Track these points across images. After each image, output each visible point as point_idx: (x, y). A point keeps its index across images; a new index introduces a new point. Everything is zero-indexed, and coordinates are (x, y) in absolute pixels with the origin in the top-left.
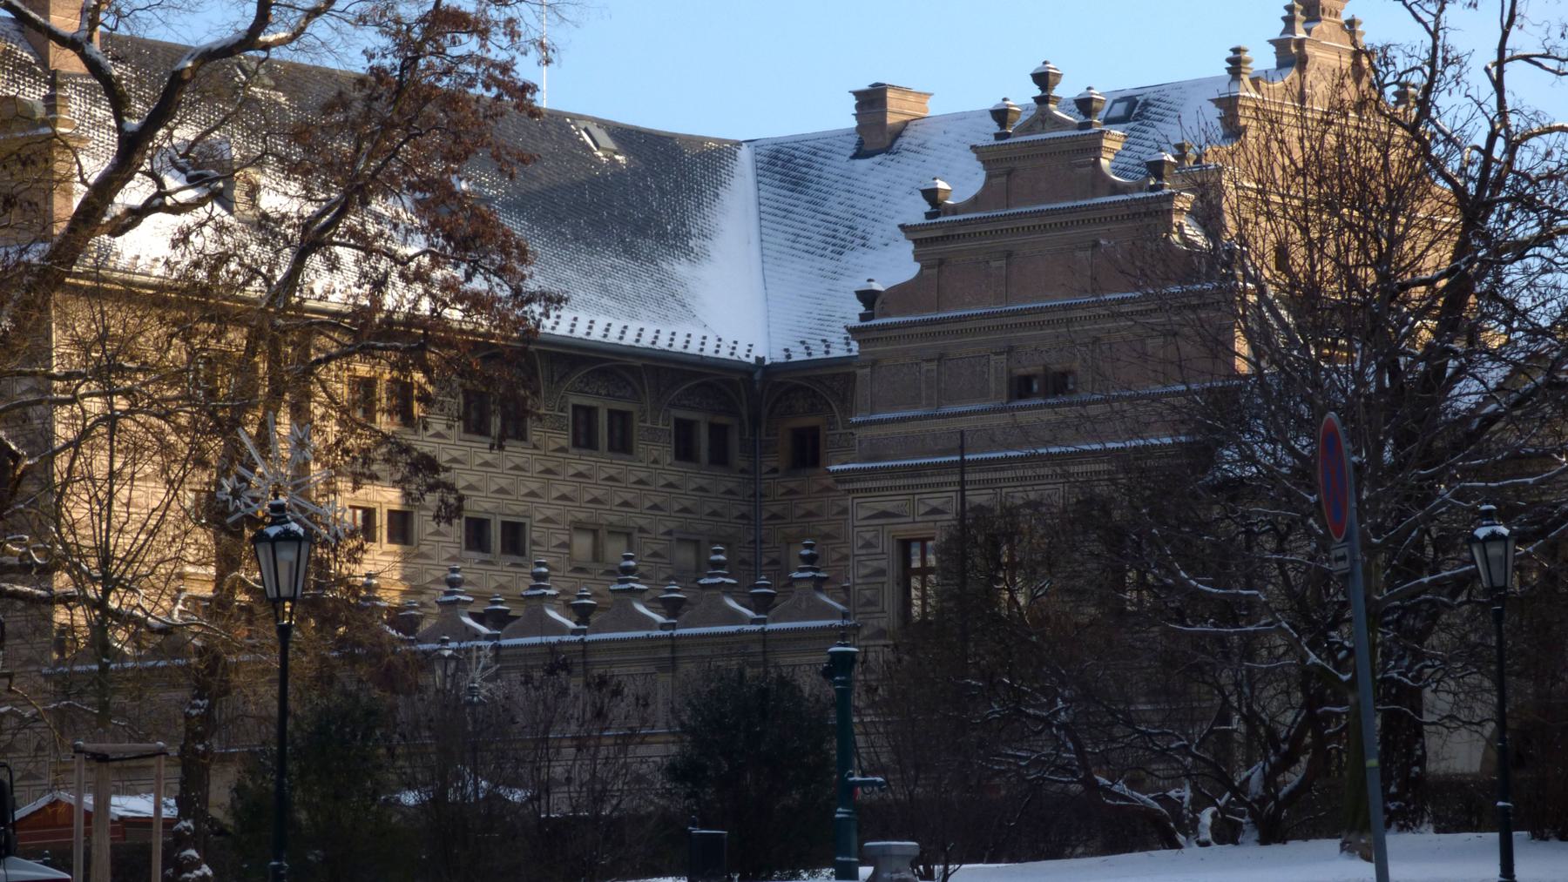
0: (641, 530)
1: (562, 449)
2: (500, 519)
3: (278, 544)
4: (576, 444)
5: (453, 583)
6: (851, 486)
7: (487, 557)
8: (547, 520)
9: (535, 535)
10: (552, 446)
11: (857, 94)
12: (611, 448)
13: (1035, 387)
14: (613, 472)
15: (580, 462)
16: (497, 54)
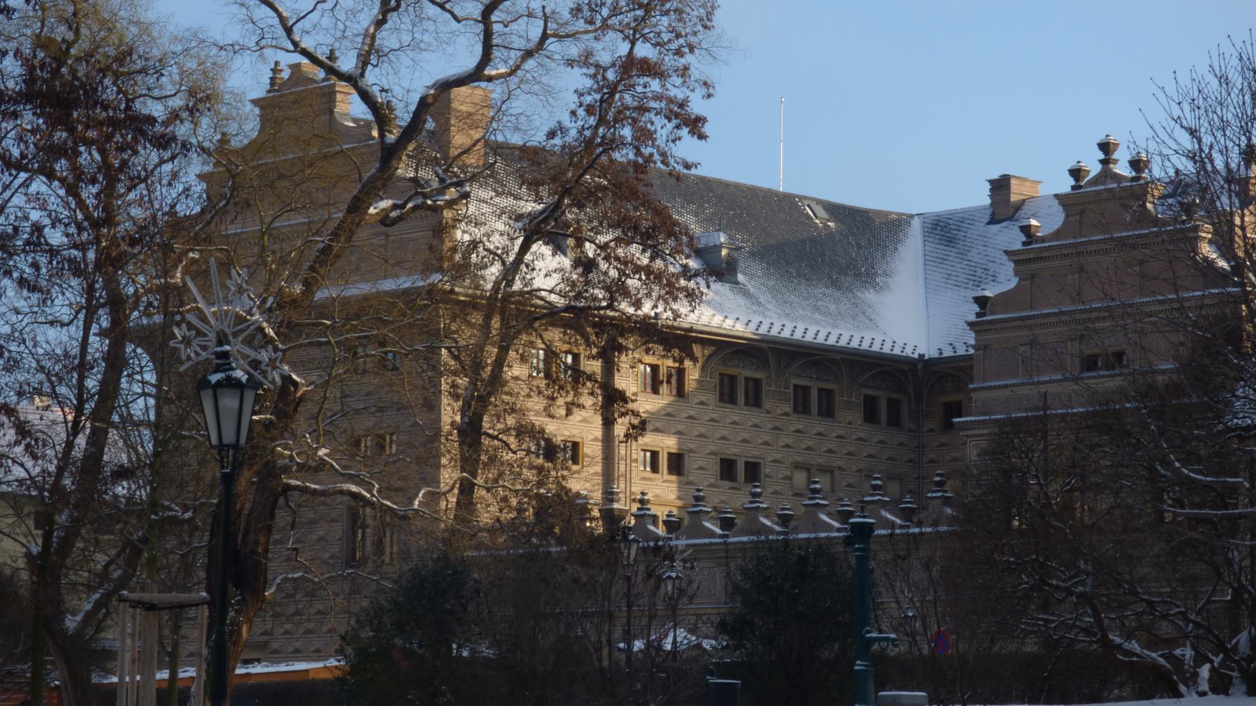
0: (840, 469)
1: (786, 414)
2: (743, 459)
3: (219, 391)
4: (796, 410)
5: (698, 499)
6: (969, 433)
7: (734, 485)
8: (776, 461)
9: (767, 471)
10: (779, 412)
11: (991, 182)
12: (820, 414)
13: (1100, 363)
14: (821, 430)
15: (799, 423)
16: (678, 93)
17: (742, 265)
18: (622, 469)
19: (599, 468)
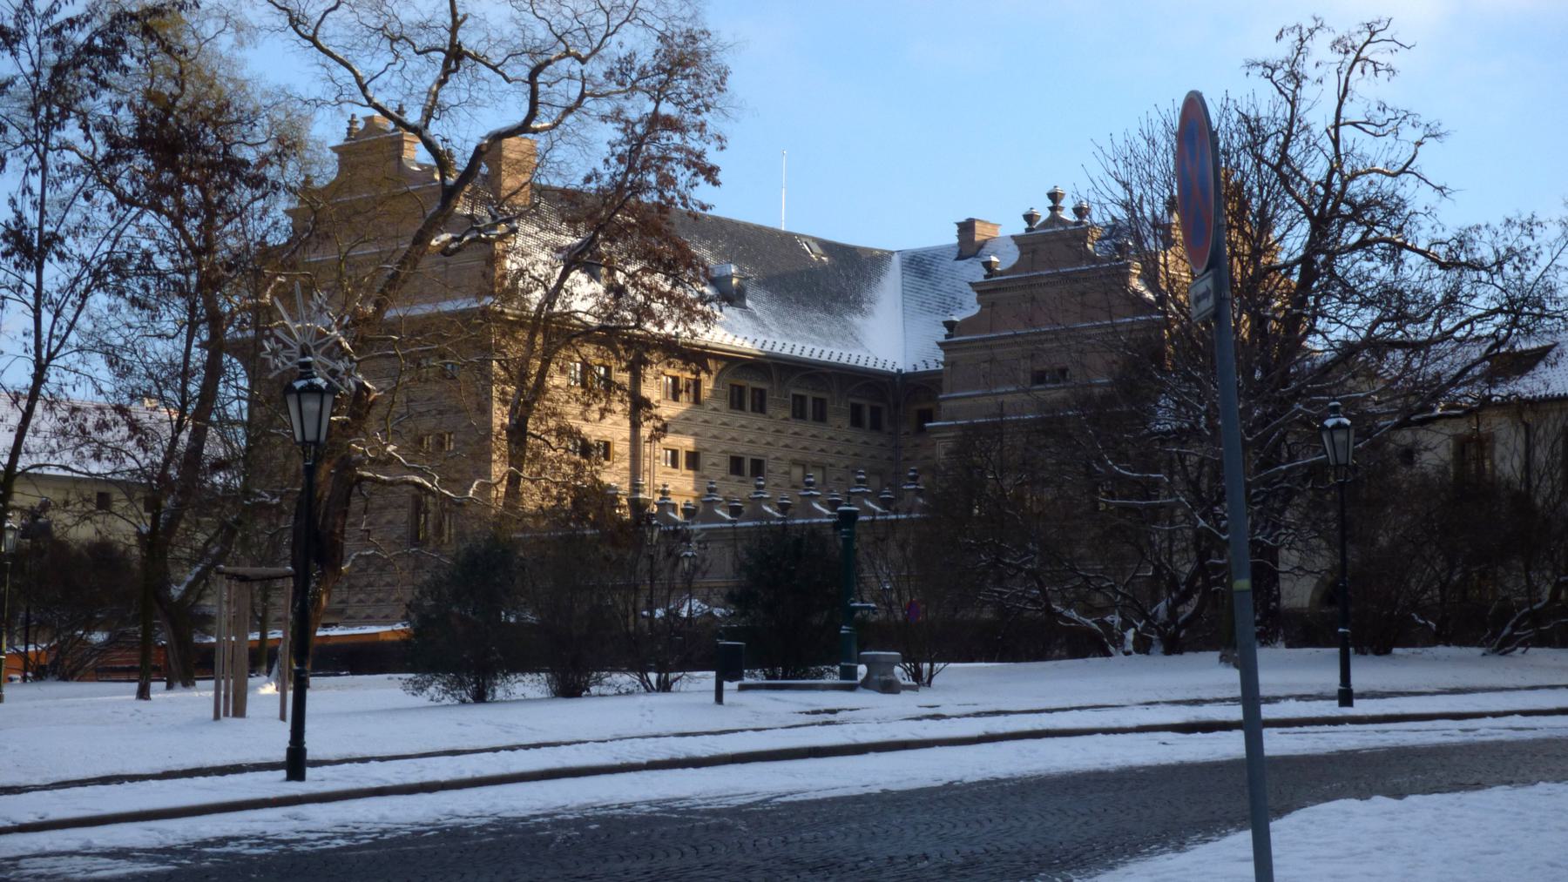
0: (831, 465)
1: (786, 419)
3: (303, 396)
4: (794, 416)
5: (711, 490)
8: (777, 458)
10: (780, 417)
11: (959, 224)
15: (797, 426)
16: (695, 145)
17: (749, 292)
18: (647, 465)
19: (627, 464)
